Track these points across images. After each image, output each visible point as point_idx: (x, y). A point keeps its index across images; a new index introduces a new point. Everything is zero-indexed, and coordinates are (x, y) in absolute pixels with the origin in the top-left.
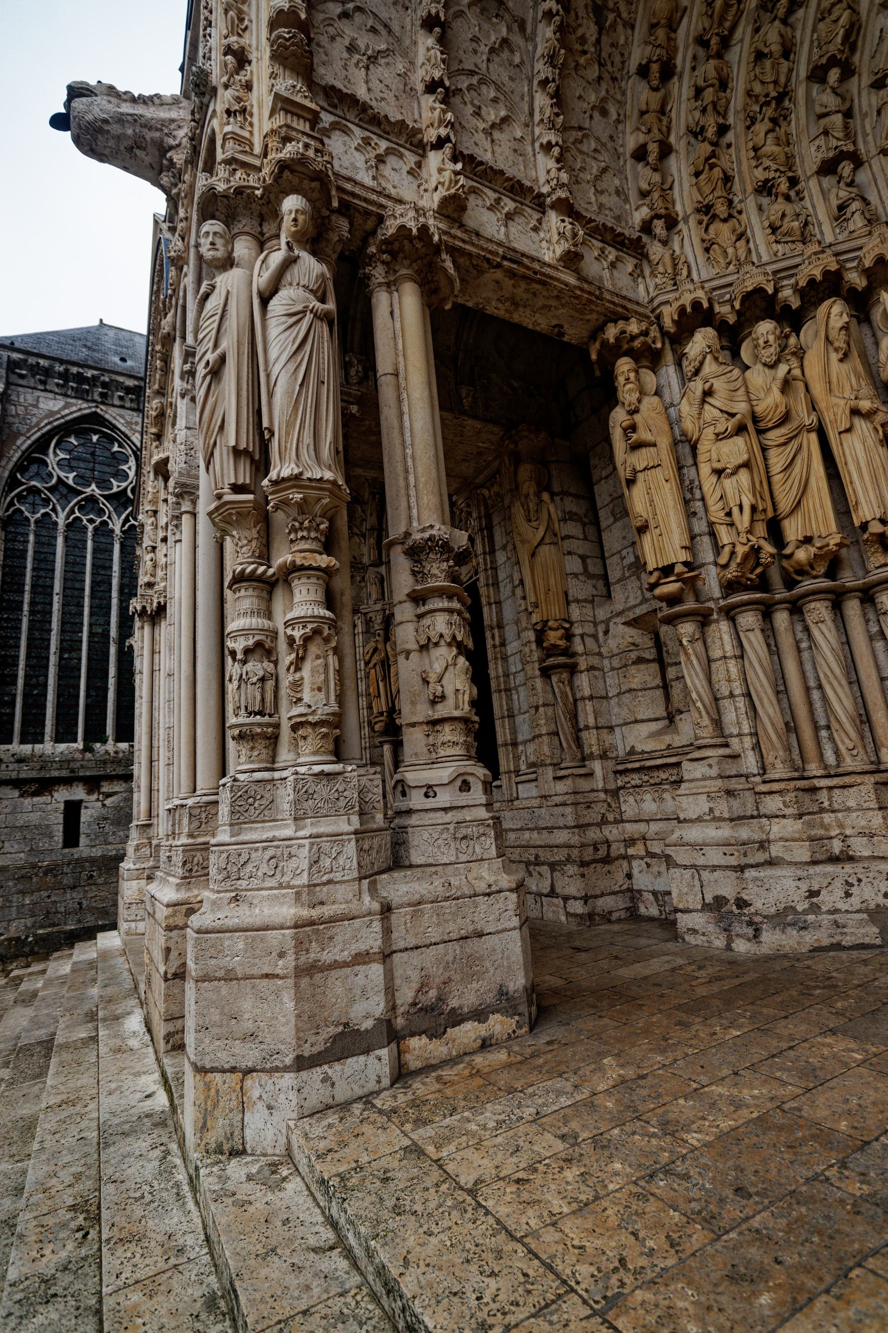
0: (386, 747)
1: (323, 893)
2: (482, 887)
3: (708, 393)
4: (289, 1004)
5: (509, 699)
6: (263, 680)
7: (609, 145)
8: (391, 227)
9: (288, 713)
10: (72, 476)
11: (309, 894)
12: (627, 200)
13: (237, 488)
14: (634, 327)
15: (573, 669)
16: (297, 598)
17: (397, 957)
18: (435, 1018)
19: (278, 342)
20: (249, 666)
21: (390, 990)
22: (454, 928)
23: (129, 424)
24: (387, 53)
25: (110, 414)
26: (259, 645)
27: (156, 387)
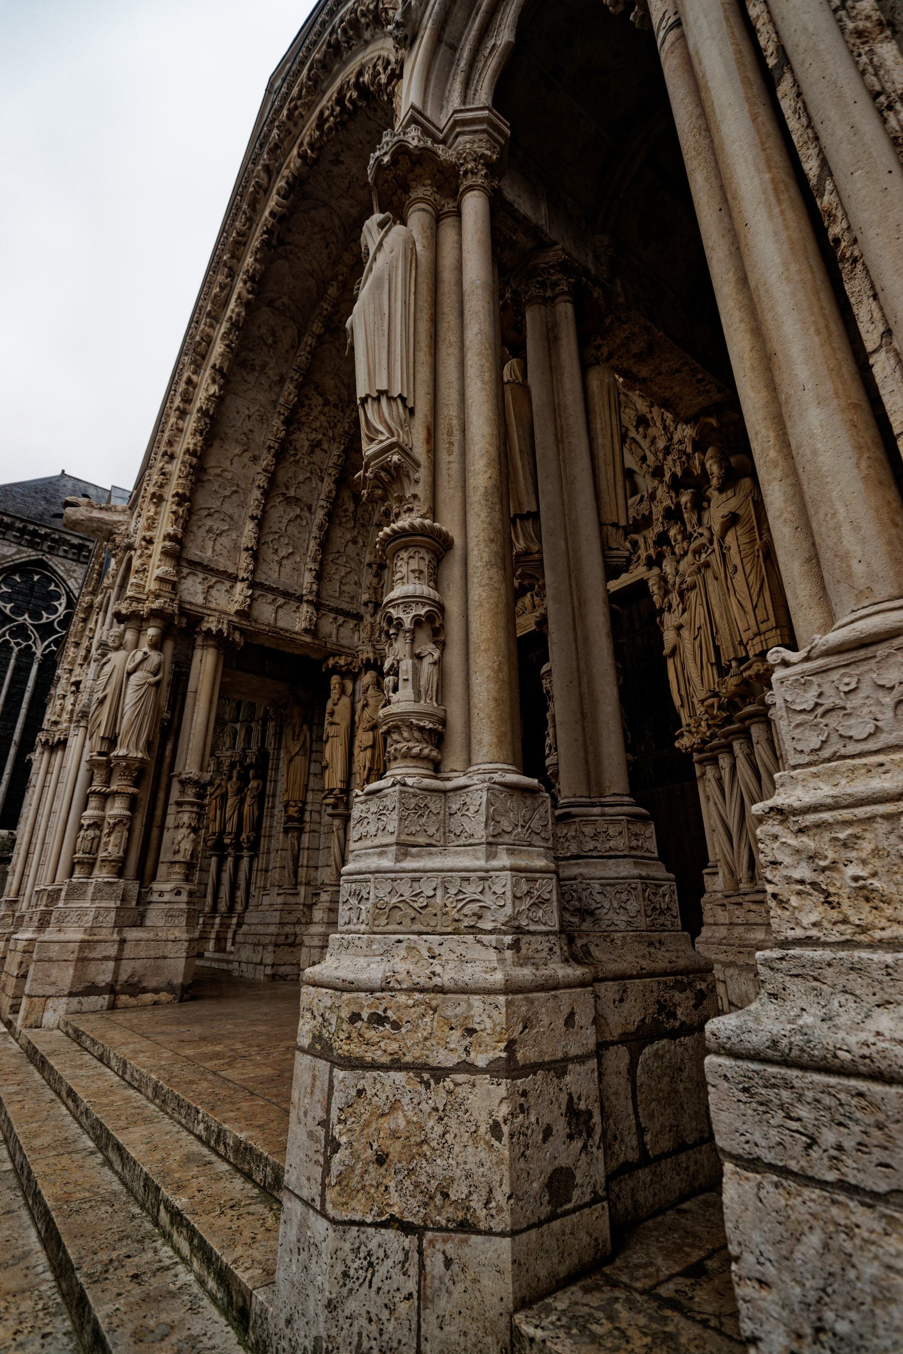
0: (214, 859)
1: (96, 931)
2: (171, 937)
3: (366, 705)
4: (71, 972)
5: (270, 841)
6: (93, 839)
7: (356, 558)
8: (205, 626)
9: (102, 854)
10: (9, 606)
11: (91, 930)
12: (361, 587)
13: (100, 754)
14: (342, 662)
15: (301, 831)
16: (116, 805)
17: (123, 962)
18: (135, 988)
19: (130, 697)
20: (88, 832)
21: (116, 973)
22: (152, 953)
23: (67, 571)
24: (229, 530)
25: (54, 562)
26: (95, 823)
27: (90, 589)
